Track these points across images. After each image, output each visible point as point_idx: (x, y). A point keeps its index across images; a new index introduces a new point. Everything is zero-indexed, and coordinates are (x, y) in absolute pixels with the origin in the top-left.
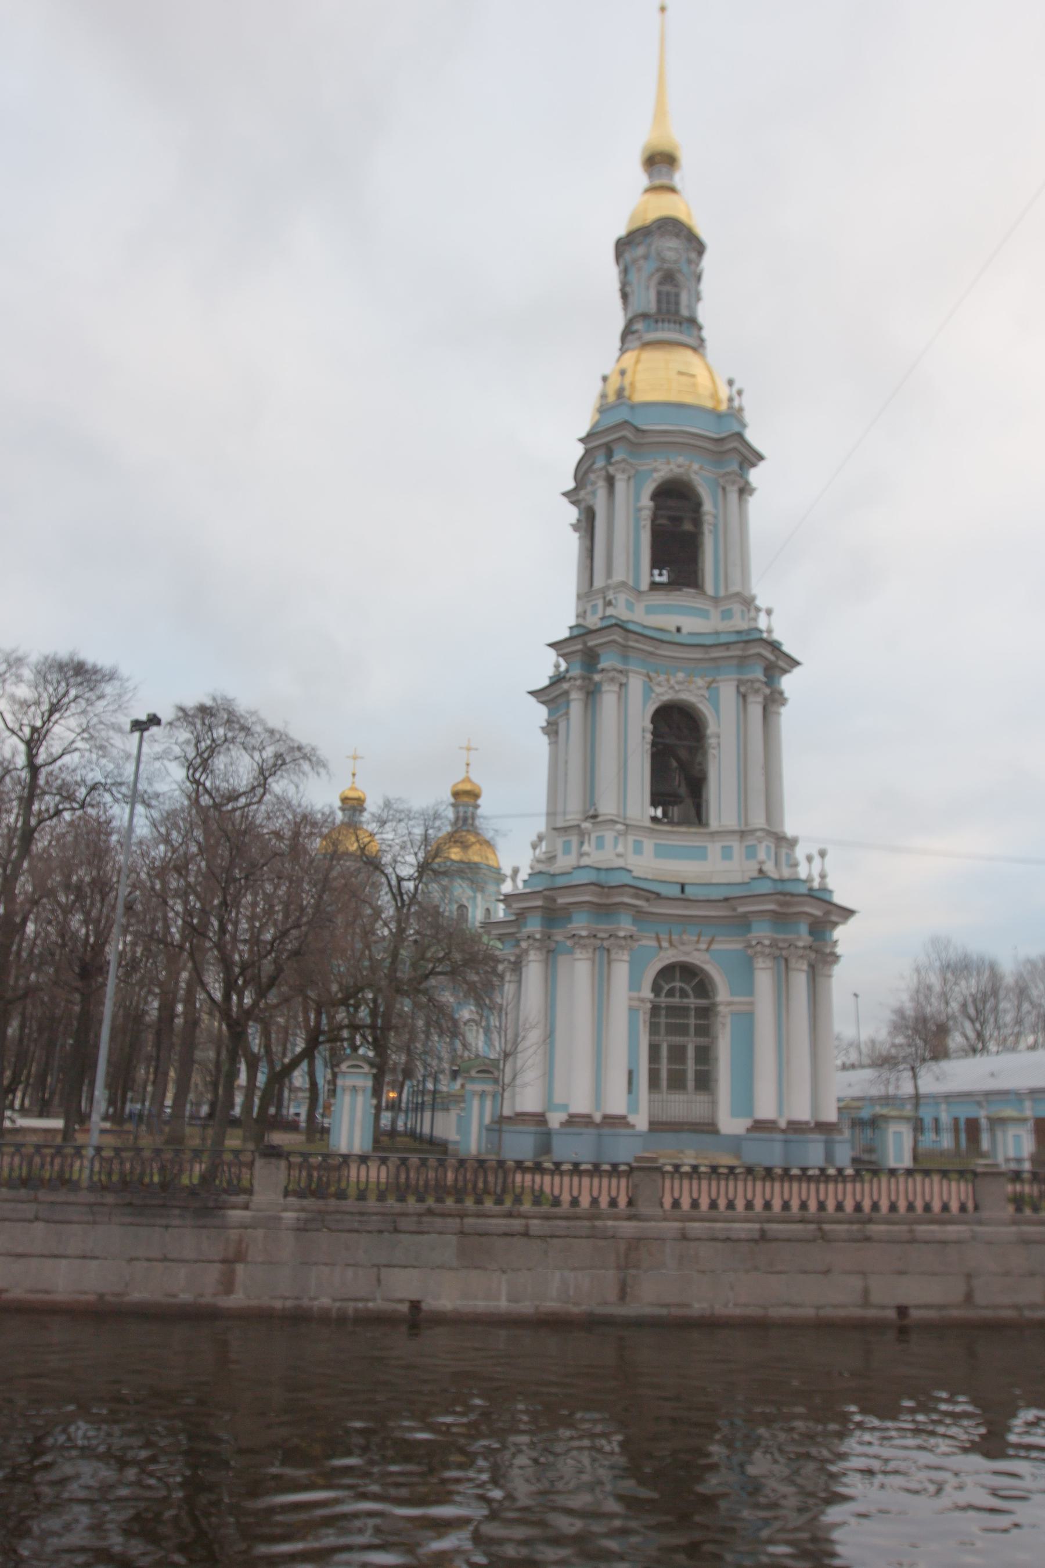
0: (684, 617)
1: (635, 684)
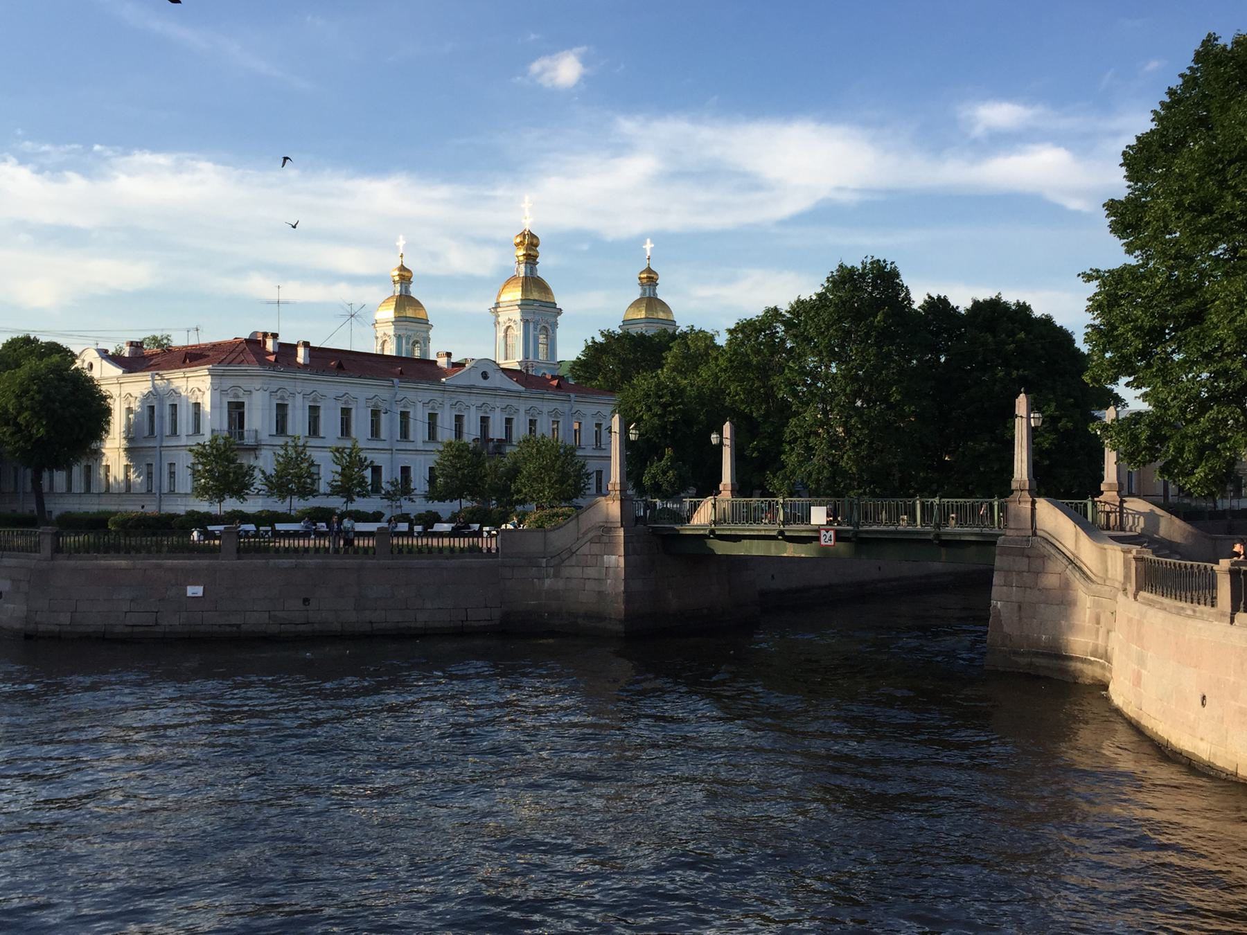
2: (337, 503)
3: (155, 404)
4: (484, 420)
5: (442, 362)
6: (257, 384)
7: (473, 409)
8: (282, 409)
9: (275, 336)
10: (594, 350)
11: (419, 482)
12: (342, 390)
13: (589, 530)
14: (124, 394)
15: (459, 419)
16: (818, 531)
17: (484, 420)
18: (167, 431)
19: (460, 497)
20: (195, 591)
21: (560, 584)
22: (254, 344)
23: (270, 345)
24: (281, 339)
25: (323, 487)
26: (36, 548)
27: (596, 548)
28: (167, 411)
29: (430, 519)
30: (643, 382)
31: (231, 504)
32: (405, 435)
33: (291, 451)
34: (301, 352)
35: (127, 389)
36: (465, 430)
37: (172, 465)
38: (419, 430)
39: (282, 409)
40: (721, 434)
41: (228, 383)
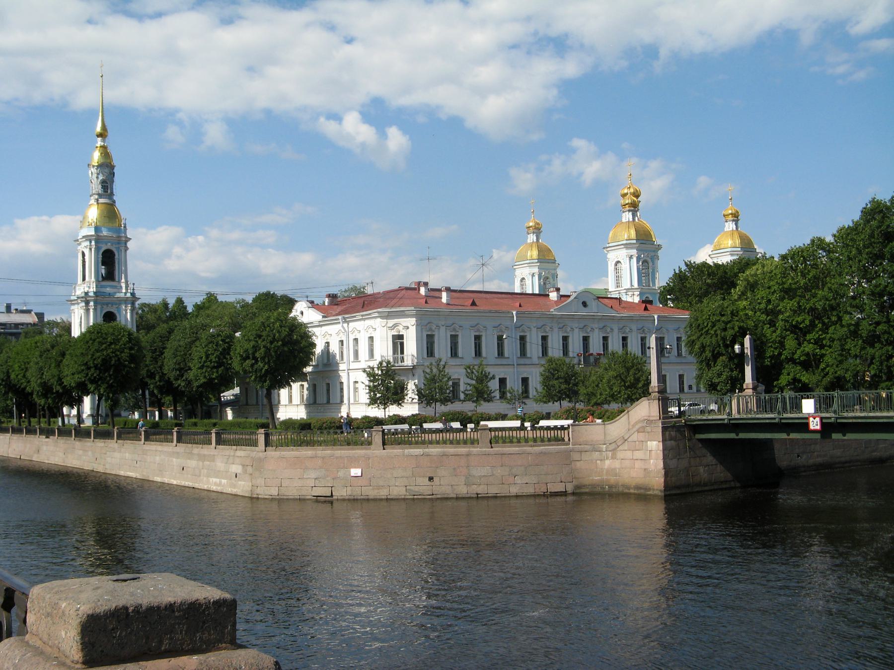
2: (468, 407)
3: (344, 338)
4: (586, 339)
7: (576, 330)
9: (426, 284)
10: (680, 278)
13: (636, 423)
16: (807, 418)
17: (586, 339)
19: (560, 399)
20: (356, 472)
21: (616, 464)
24: (431, 286)
26: (255, 444)
27: (641, 436)
30: (713, 304)
31: (393, 410)
32: (523, 353)
33: (435, 370)
34: (444, 295)
36: (570, 348)
38: (534, 349)
40: (742, 345)
41: (391, 322)
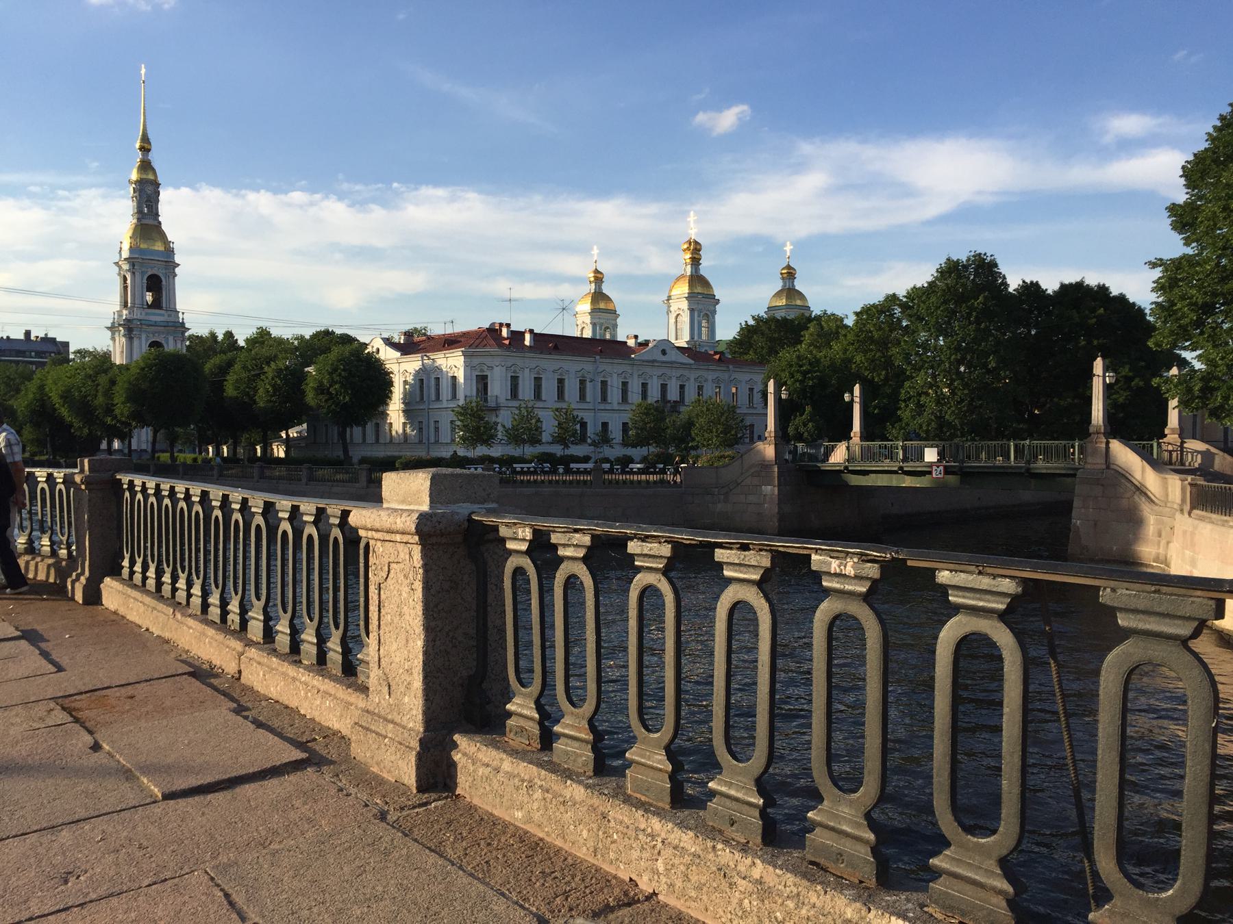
0: (157, 316)
1: (144, 336)
2: (557, 450)
4: (664, 387)
5: (631, 343)
6: (497, 361)
8: (515, 380)
9: (508, 325)
10: (748, 332)
11: (616, 433)
12: (556, 365)
14: (403, 370)
15: (644, 385)
17: (664, 387)
18: (433, 397)
19: (649, 444)
22: (493, 332)
23: (505, 332)
24: (513, 328)
25: (545, 437)
28: (433, 382)
29: (626, 461)
30: (787, 355)
31: (481, 451)
32: (604, 399)
33: (524, 411)
35: (404, 366)
36: (649, 393)
37: (436, 422)
38: (614, 395)
39: (515, 380)
40: (852, 393)
41: (476, 361)
